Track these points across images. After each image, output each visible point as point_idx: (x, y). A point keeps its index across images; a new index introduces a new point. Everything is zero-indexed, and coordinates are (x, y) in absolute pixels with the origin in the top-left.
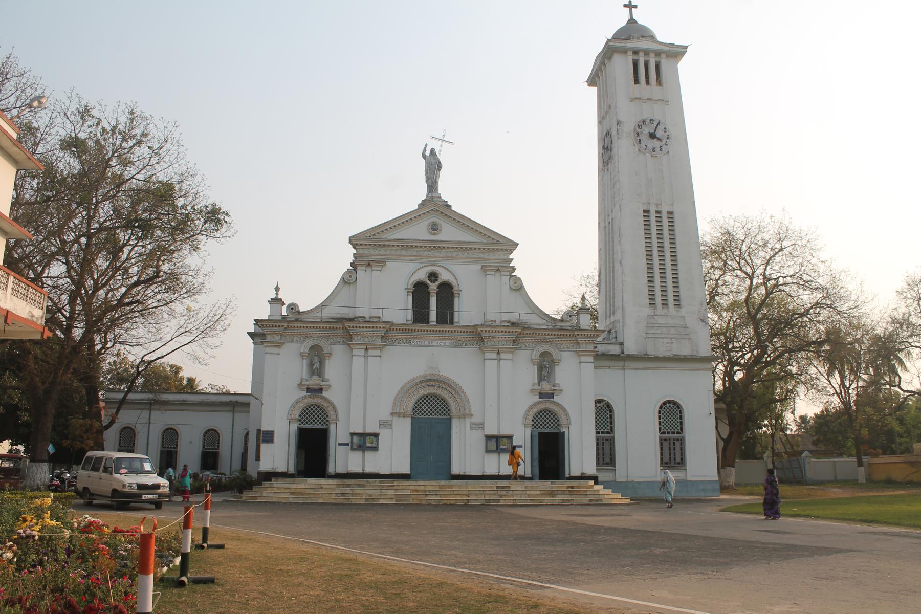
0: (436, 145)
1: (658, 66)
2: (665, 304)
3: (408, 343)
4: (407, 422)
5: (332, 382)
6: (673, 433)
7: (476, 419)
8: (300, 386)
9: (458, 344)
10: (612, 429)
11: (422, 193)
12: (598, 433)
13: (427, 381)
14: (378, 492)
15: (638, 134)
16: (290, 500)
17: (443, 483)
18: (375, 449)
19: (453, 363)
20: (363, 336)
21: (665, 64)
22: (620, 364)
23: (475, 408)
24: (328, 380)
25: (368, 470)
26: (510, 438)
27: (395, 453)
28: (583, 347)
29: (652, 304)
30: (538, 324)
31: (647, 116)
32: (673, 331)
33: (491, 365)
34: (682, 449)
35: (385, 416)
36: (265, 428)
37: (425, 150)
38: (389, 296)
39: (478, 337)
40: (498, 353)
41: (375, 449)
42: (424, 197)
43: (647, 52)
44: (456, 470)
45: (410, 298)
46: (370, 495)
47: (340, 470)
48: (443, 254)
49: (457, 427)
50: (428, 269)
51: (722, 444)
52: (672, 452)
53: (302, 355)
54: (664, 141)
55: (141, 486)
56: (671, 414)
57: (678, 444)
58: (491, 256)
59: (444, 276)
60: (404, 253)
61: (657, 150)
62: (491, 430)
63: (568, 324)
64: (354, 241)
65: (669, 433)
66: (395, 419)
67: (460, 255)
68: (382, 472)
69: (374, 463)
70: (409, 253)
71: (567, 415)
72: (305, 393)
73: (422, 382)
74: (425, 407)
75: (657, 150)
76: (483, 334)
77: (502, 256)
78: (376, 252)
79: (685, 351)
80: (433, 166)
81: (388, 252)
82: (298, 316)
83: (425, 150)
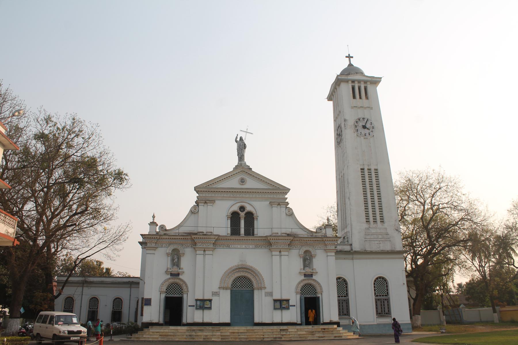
2: (375, 221)
3: (228, 247)
4: (229, 292)
5: (184, 270)
6: (383, 296)
7: (268, 290)
8: (166, 272)
9: (257, 247)
10: (347, 294)
11: (235, 162)
12: (339, 297)
13: (240, 268)
14: (211, 334)
15: (356, 126)
16: (159, 339)
17: (249, 328)
18: (210, 308)
19: (254, 258)
20: (202, 243)
21: (370, 88)
22: (351, 256)
23: (267, 283)
24: (182, 269)
25: (206, 320)
26: (288, 301)
27: (221, 311)
28: (329, 247)
29: (368, 221)
30: (302, 235)
31: (361, 116)
32: (380, 237)
33: (276, 259)
34: (389, 305)
35: (216, 289)
36: (146, 297)
37: (237, 138)
39: (268, 242)
40: (280, 252)
41: (210, 308)
42: (237, 164)
43: (359, 82)
44: (257, 320)
46: (206, 336)
47: (190, 321)
48: (247, 196)
49: (257, 294)
50: (239, 205)
51: (412, 301)
52: (383, 306)
53: (168, 254)
54: (371, 130)
55: (70, 332)
56: (381, 285)
57: (386, 302)
58: (275, 196)
59: (249, 208)
60: (225, 195)
61: (367, 134)
62: (277, 297)
63: (320, 234)
64: (197, 189)
65: (380, 296)
66: (222, 292)
67: (258, 196)
68: (214, 322)
69: (209, 317)
70: (229, 195)
71: (321, 286)
72: (169, 276)
73: (236, 269)
75: (367, 134)
76: (271, 241)
77: (281, 197)
78: (210, 195)
79: (388, 247)
80: (241, 146)
81: (216, 195)
82: (165, 232)
83: (237, 138)
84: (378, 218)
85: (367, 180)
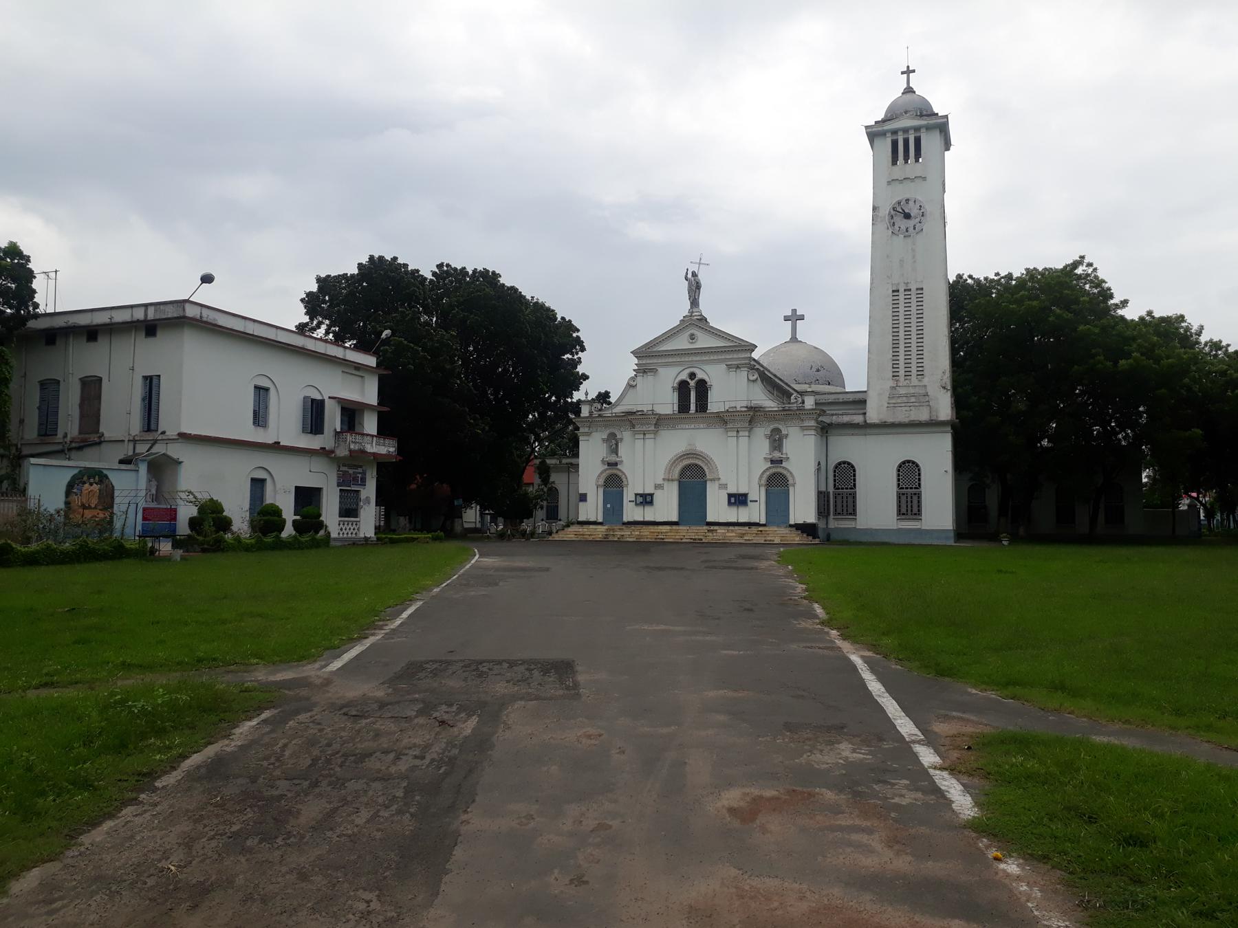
0: (694, 268)
3: (674, 428)
7: (723, 481)
8: (603, 461)
11: (683, 308)
25: (647, 519)
26: (746, 495)
27: (667, 507)
32: (913, 399)
33: (744, 441)
34: (919, 502)
35: (660, 481)
38: (660, 395)
39: (723, 420)
42: (686, 313)
44: (709, 519)
45: (676, 394)
50: (688, 371)
56: (909, 473)
57: (915, 498)
59: (700, 375)
62: (733, 490)
66: (666, 483)
68: (658, 520)
69: (649, 514)
74: (688, 473)
75: (911, 229)
79: (923, 416)
85: (902, 309)
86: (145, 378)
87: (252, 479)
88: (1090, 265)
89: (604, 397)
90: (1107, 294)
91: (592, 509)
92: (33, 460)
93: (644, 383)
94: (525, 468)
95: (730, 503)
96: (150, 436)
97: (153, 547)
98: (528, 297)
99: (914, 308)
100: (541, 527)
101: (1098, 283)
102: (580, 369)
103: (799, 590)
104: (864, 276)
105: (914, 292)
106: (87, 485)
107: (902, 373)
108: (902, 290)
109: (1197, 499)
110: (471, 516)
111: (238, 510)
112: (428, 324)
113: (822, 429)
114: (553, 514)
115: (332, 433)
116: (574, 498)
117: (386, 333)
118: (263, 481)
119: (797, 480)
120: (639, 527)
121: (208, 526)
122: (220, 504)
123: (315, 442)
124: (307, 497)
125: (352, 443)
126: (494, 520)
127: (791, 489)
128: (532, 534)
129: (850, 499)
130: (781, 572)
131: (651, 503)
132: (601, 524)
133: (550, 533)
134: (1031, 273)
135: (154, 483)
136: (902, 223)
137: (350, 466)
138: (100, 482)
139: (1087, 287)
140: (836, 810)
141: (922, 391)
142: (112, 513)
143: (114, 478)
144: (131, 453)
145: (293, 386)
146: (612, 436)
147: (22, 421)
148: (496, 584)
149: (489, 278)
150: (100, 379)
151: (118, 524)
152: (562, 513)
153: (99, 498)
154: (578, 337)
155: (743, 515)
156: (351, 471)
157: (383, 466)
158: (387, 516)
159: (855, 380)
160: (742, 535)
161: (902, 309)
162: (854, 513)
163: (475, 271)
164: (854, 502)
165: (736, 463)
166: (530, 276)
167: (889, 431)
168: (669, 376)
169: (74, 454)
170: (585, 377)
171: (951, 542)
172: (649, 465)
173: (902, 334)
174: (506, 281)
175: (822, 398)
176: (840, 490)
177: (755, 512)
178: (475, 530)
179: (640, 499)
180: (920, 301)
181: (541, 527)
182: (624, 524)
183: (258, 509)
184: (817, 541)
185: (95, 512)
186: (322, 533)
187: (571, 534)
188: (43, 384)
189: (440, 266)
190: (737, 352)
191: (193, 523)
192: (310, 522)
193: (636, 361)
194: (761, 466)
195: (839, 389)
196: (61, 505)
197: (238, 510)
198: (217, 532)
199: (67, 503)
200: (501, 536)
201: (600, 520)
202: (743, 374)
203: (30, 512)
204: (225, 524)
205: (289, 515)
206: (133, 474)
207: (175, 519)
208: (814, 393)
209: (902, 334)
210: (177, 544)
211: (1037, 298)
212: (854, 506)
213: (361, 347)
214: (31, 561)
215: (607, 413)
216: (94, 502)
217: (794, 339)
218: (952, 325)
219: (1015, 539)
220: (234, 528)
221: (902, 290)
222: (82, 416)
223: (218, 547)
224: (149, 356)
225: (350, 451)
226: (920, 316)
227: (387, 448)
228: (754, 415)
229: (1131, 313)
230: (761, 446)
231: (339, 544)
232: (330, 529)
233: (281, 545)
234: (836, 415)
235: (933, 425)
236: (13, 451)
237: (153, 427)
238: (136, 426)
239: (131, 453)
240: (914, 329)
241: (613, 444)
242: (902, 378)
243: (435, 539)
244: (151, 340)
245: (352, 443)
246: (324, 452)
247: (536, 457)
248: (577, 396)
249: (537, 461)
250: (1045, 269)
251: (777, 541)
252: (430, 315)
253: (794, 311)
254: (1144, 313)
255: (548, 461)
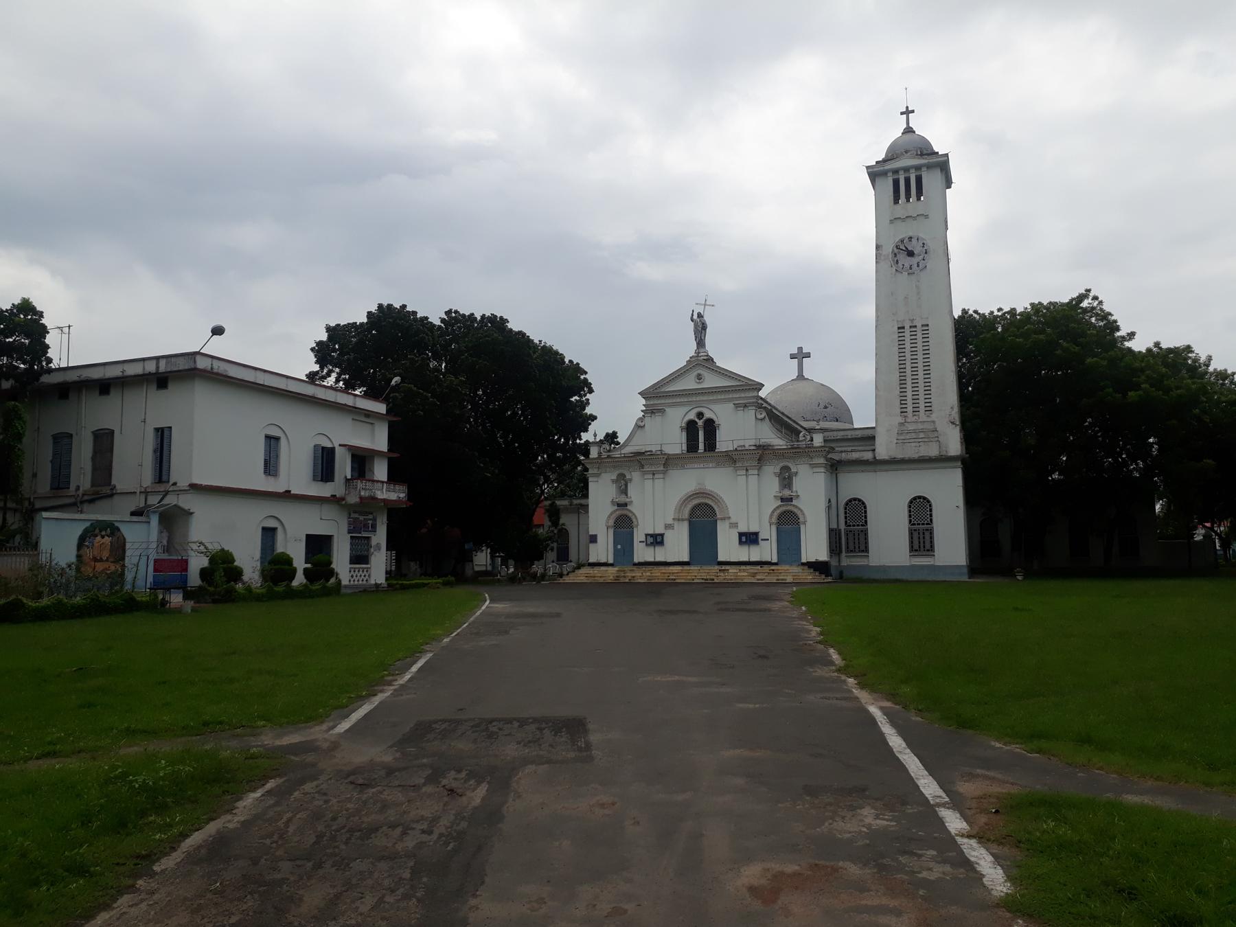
1: (919, 180)
3: (683, 467)
4: (685, 525)
7: (733, 520)
8: (613, 502)
9: (718, 465)
11: (691, 348)
25: (658, 559)
26: (756, 534)
27: (678, 547)
32: (922, 435)
34: (932, 538)
35: (670, 521)
38: (669, 435)
39: (732, 459)
43: (906, 170)
44: (721, 558)
45: (684, 434)
52: (922, 539)
53: (613, 481)
56: (920, 509)
62: (743, 529)
69: (660, 555)
79: (932, 451)
84: (922, 405)
85: (908, 346)
86: (157, 430)
87: (264, 529)
88: (1095, 298)
89: (611, 437)
90: (1114, 327)
91: (602, 550)
92: (45, 514)
93: (652, 423)
94: (534, 510)
95: (741, 542)
96: (162, 488)
97: (163, 599)
98: (536, 341)
99: (920, 345)
100: (552, 568)
101: (1105, 316)
102: (588, 411)
103: (814, 634)
104: (868, 311)
105: (919, 328)
106: (99, 538)
107: (910, 409)
108: (907, 327)
109: (1212, 529)
110: (482, 559)
111: (249, 560)
112: (437, 370)
113: (832, 466)
114: (563, 556)
115: (343, 481)
116: (584, 539)
117: (396, 380)
118: (274, 530)
119: (809, 519)
120: (650, 568)
121: (219, 576)
122: (231, 555)
123: (325, 490)
124: (318, 545)
125: (363, 490)
126: (505, 562)
127: (802, 527)
128: (543, 577)
129: (862, 537)
130: (795, 614)
131: (661, 543)
132: (612, 565)
133: (561, 575)
134: (1037, 307)
135: (165, 535)
136: (907, 261)
137: (361, 513)
138: (112, 535)
139: (1093, 320)
140: (861, 887)
141: (931, 427)
142: (123, 566)
143: (126, 530)
144: (142, 504)
145: (304, 435)
146: (622, 476)
147: (35, 475)
148: (507, 632)
149: (497, 324)
150: (113, 432)
151: (129, 576)
152: (573, 554)
153: (111, 551)
154: (586, 379)
155: (754, 554)
156: (362, 518)
157: (393, 511)
158: (398, 561)
159: (863, 417)
160: (754, 575)
161: (908, 346)
162: (866, 550)
163: (483, 317)
164: (866, 539)
165: (746, 502)
166: (535, 319)
167: (899, 466)
168: (677, 416)
169: (86, 507)
170: (594, 418)
171: (965, 578)
172: (658, 505)
173: (908, 370)
174: (514, 325)
175: (831, 435)
176: (851, 528)
177: (767, 551)
178: (486, 573)
179: (650, 540)
180: (926, 337)
181: (552, 568)
182: (635, 564)
183: (269, 558)
184: (829, 579)
185: (106, 565)
186: (333, 580)
187: (581, 576)
188: (57, 438)
189: (448, 313)
190: (744, 391)
191: (204, 573)
192: (320, 568)
193: (644, 402)
194: (772, 504)
195: (847, 426)
196: (73, 559)
197: (249, 560)
198: (228, 582)
199: (79, 556)
200: (512, 579)
201: (611, 561)
202: (751, 413)
203: (41, 567)
204: (236, 574)
205: (300, 563)
206: (145, 526)
207: (186, 570)
208: (823, 430)
209: (908, 370)
210: (188, 595)
211: (1042, 332)
212: (867, 543)
213: (370, 395)
214: (42, 616)
215: (616, 454)
216: (105, 554)
217: (801, 376)
218: (958, 360)
219: (1029, 574)
220: (245, 578)
221: (907, 327)
222: (94, 469)
223: (229, 597)
224: (160, 408)
225: (361, 498)
226: (926, 353)
227: (396, 494)
228: (762, 453)
229: (1138, 345)
230: (772, 486)
231: (349, 591)
232: (341, 577)
233: (292, 594)
234: (845, 451)
235: (943, 460)
236: (26, 504)
237: (164, 478)
238: (148, 478)
239: (142, 504)
240: (920, 365)
241: (623, 484)
242: (910, 414)
243: (446, 584)
244: (163, 393)
245: (363, 490)
246: (334, 500)
247: (546, 499)
248: (586, 437)
249: (547, 503)
250: (1050, 303)
251: (789, 579)
252: (439, 360)
253: (800, 349)
254: (1151, 345)
255: (558, 503)
